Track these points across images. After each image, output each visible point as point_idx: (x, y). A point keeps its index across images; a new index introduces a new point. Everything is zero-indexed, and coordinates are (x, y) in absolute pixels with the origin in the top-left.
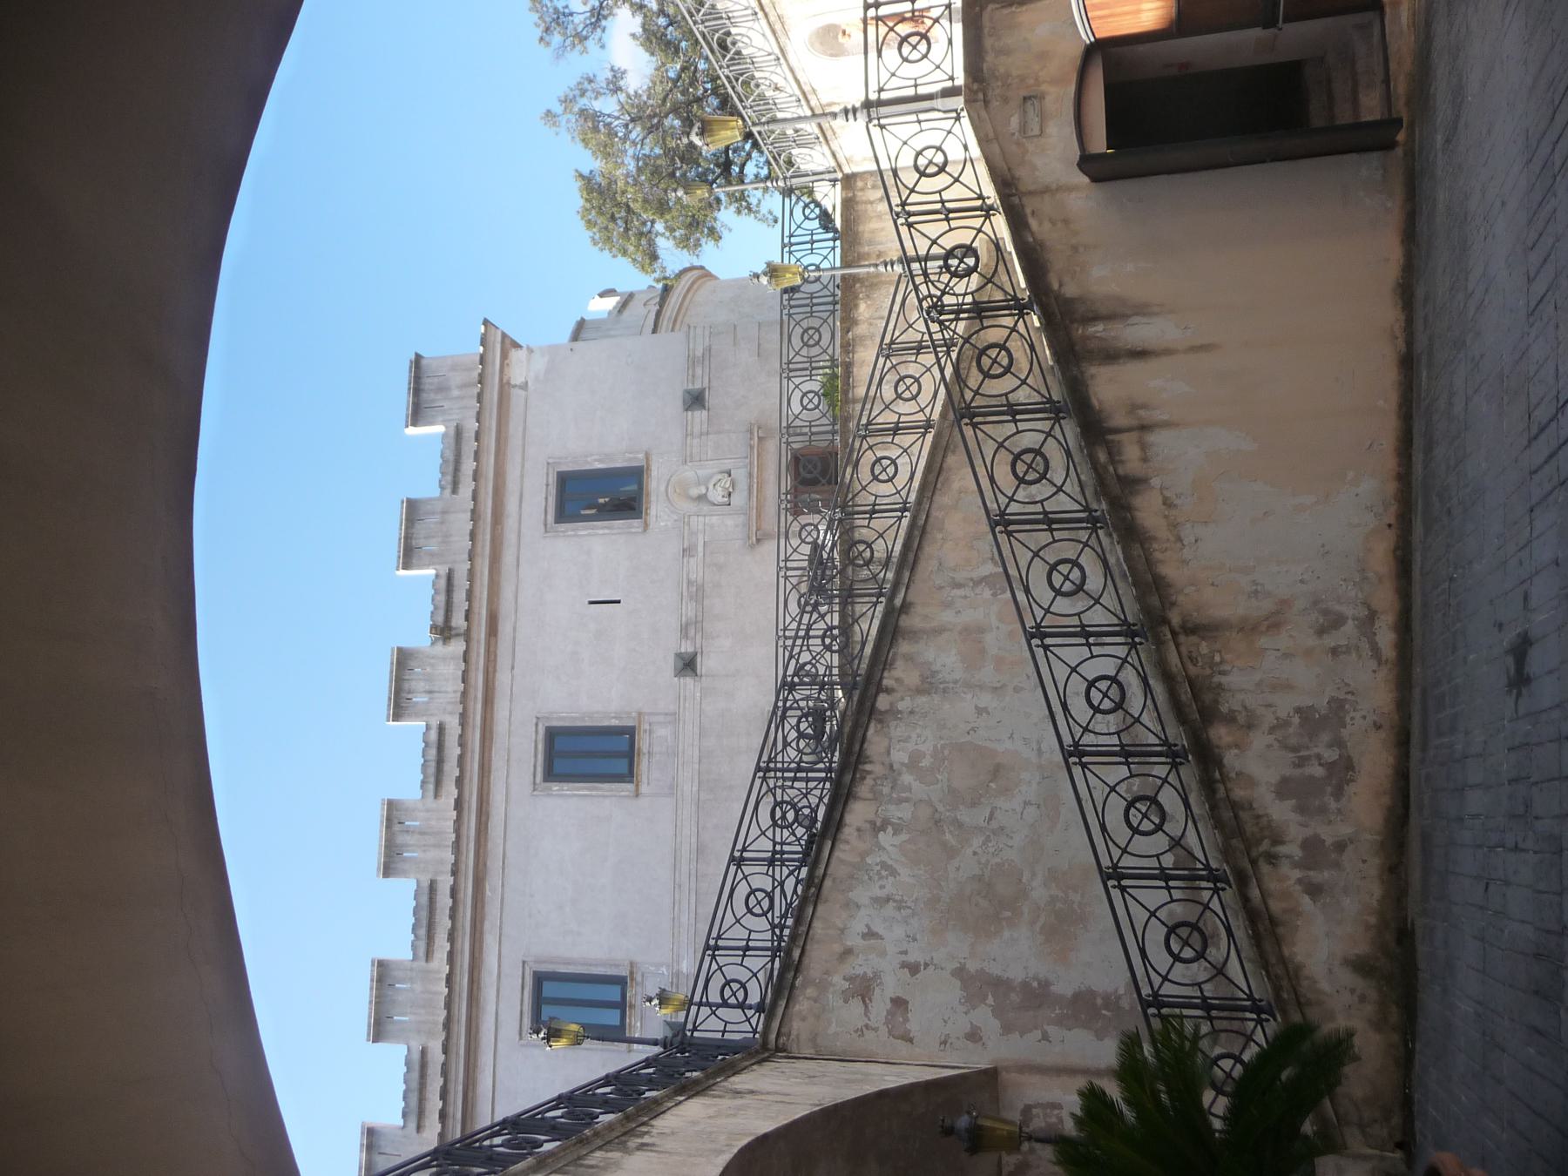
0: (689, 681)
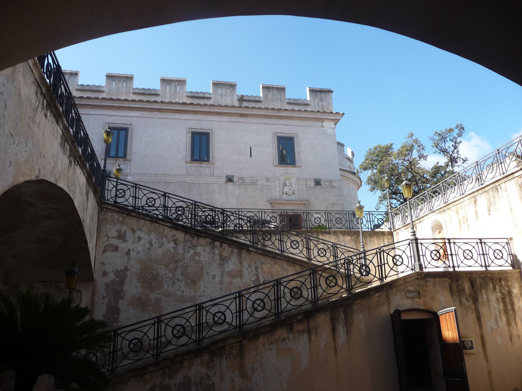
0: (225, 180)
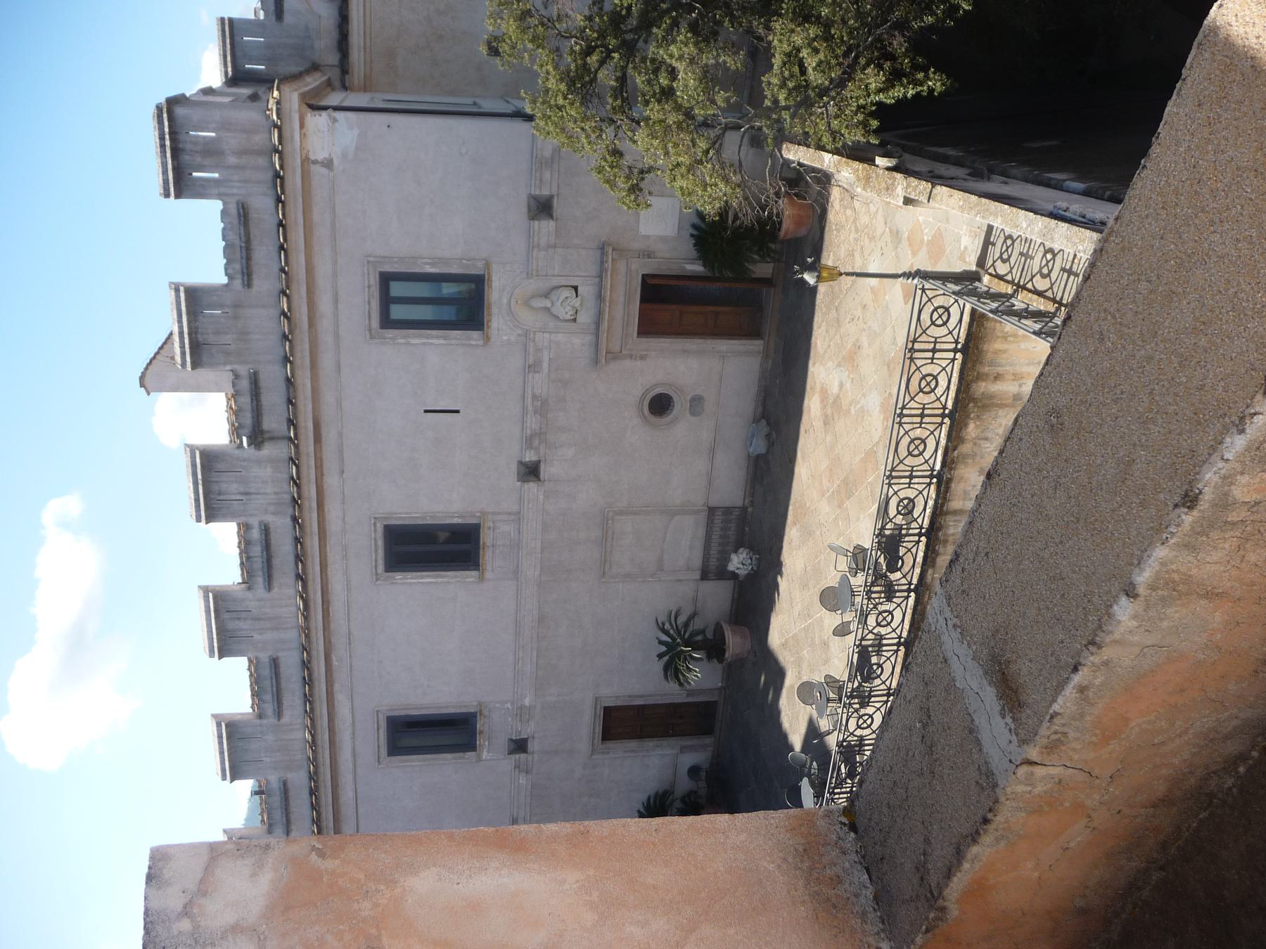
0: (532, 486)
